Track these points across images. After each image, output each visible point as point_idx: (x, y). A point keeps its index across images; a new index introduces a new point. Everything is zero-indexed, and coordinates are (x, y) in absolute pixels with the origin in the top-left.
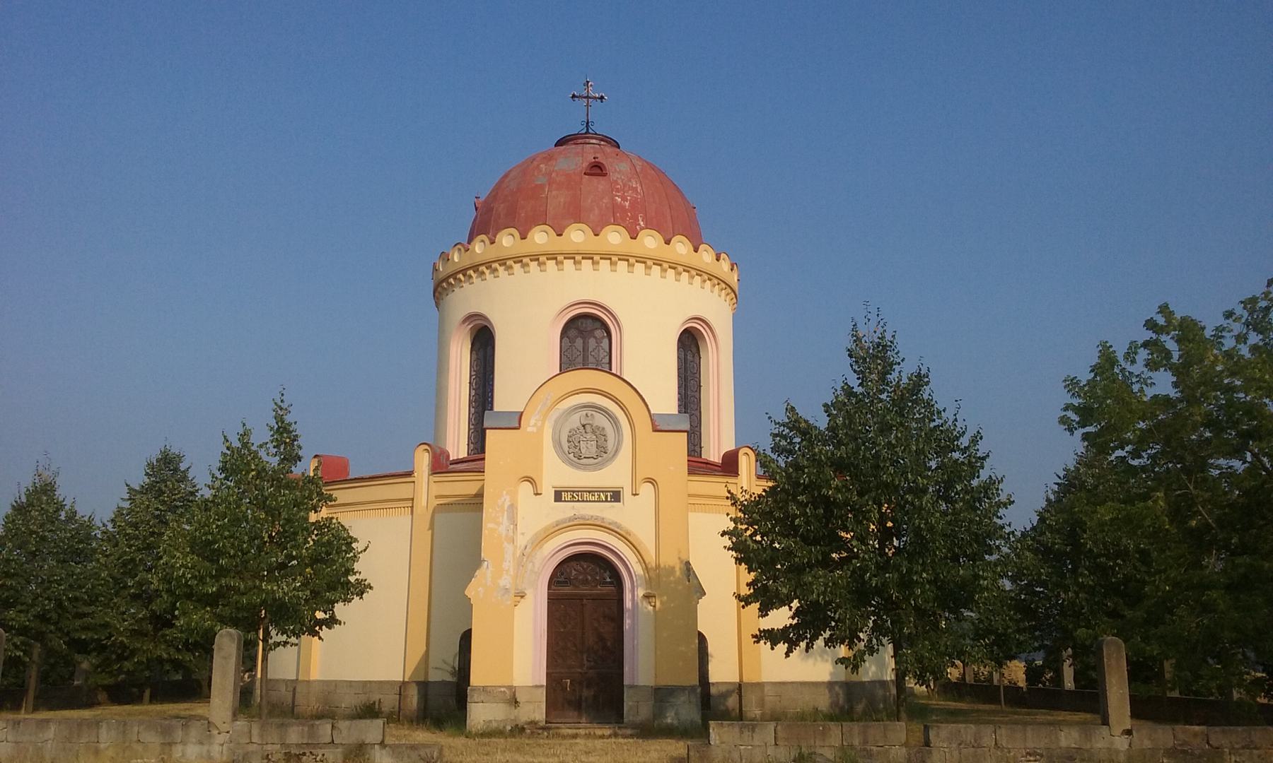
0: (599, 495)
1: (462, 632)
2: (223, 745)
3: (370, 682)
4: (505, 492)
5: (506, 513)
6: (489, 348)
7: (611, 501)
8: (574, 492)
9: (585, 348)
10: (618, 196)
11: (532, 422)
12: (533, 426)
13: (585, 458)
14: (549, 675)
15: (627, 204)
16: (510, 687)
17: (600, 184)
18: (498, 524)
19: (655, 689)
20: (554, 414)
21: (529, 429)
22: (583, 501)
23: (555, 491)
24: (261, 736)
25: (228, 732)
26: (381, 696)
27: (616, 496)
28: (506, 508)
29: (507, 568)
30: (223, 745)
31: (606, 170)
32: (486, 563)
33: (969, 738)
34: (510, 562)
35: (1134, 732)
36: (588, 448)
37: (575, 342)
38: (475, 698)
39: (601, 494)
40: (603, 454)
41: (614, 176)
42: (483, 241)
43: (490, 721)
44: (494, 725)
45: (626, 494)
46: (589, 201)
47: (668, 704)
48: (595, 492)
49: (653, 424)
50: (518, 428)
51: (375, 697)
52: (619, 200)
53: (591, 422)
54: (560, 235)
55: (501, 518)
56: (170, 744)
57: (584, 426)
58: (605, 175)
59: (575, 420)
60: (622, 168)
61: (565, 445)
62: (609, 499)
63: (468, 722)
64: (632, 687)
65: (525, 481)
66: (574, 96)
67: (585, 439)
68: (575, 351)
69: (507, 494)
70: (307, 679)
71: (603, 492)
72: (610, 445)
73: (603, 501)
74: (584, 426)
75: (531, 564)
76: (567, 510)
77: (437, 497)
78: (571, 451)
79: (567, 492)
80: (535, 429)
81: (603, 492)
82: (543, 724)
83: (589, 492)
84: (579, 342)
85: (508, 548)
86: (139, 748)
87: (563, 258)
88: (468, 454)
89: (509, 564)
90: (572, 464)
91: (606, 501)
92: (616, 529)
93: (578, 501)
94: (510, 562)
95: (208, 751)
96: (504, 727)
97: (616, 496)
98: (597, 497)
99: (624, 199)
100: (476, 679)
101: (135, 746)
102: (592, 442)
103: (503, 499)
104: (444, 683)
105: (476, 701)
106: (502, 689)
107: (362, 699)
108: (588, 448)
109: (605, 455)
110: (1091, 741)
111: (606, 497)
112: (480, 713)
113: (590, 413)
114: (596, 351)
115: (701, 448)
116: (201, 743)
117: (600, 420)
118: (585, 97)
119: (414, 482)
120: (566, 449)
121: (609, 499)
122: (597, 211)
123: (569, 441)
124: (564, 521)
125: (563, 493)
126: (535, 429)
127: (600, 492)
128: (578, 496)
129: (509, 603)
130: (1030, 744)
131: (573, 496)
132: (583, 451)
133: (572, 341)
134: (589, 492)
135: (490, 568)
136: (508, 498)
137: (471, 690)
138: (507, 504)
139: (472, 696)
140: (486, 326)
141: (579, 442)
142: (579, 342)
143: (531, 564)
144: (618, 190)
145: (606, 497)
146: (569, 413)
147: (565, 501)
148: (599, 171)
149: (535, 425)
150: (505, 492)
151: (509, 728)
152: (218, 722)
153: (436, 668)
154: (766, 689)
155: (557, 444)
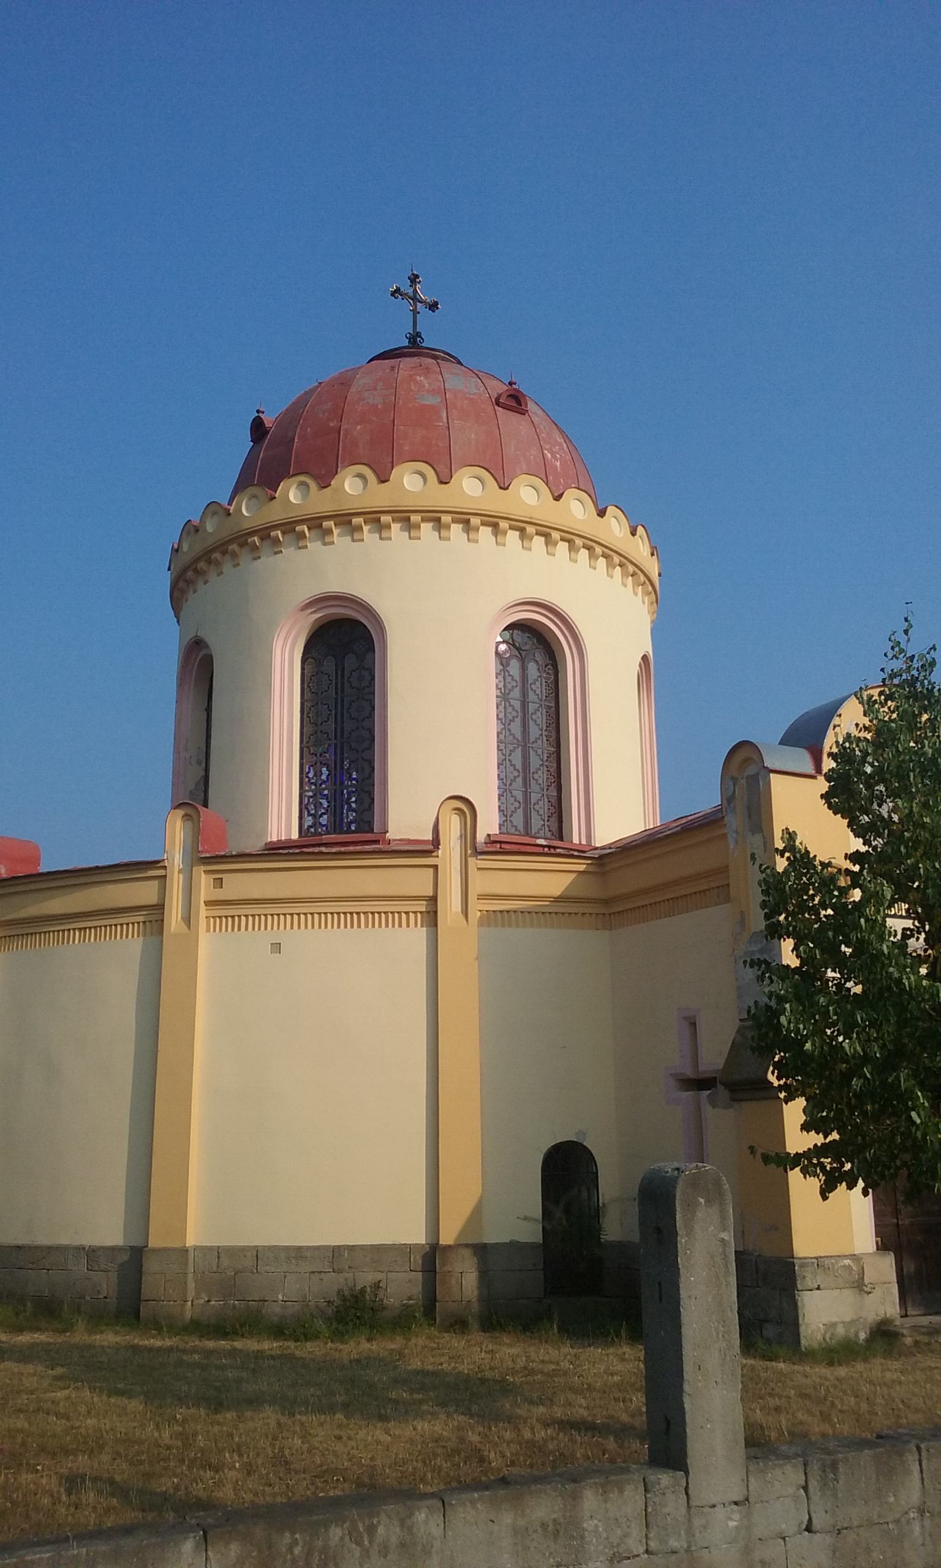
1: (545, 1150)
3: (351, 1248)
6: (350, 662)
16: (855, 1257)
26: (379, 1276)
31: (526, 406)
37: (508, 665)
38: (810, 1282)
42: (360, 476)
43: (834, 1325)
44: (841, 1331)
51: (366, 1278)
58: (523, 413)
63: (802, 1329)
68: (509, 679)
70: (177, 1245)
77: (482, 897)
96: (857, 1335)
106: (847, 1262)
107: (332, 1283)
119: (436, 867)
148: (515, 405)
151: (862, 1336)
153: (525, 1218)
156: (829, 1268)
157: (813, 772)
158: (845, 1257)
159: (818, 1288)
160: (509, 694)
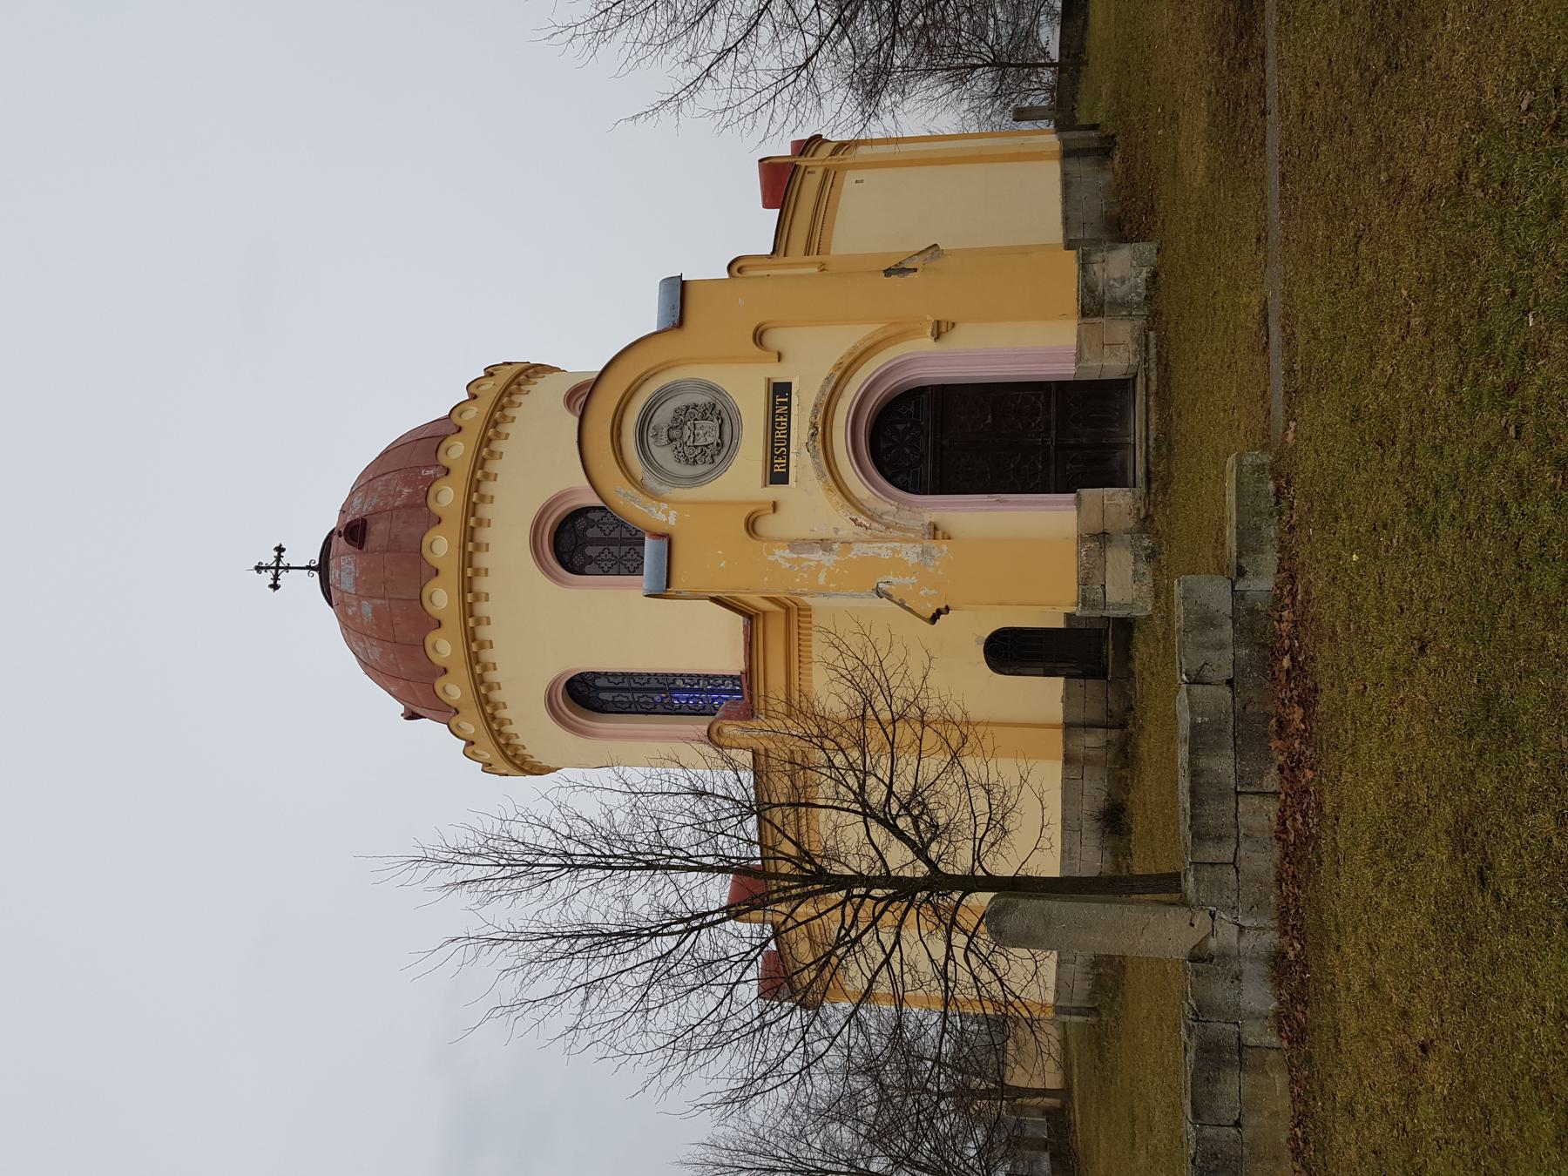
0: (780, 414)
2: (1241, 929)
4: (771, 558)
5: (803, 556)
8: (773, 454)
9: (596, 542)
11: (661, 517)
12: (667, 516)
13: (720, 438)
15: (406, 491)
16: (1081, 539)
17: (377, 533)
18: (820, 566)
20: (652, 483)
21: (672, 521)
22: (788, 439)
23: (771, 483)
24: (1220, 838)
25: (1213, 916)
27: (780, 391)
28: (796, 556)
29: (890, 551)
30: (1241, 929)
32: (880, 585)
34: (880, 548)
36: (707, 432)
37: (591, 557)
39: (777, 412)
40: (718, 412)
45: (780, 374)
47: (1108, 295)
53: (665, 430)
55: (811, 563)
56: (1241, 1047)
57: (671, 440)
59: (663, 454)
61: (700, 469)
62: (786, 400)
65: (755, 533)
67: (692, 439)
69: (773, 554)
71: (774, 410)
72: (703, 399)
75: (885, 517)
76: (801, 460)
78: (709, 459)
79: (773, 464)
80: (673, 513)
82: (1141, 490)
83: (774, 430)
84: (592, 551)
85: (858, 550)
86: (1251, 1121)
87: (469, 569)
89: (884, 551)
90: (729, 458)
91: (789, 404)
92: (833, 384)
93: (788, 447)
94: (880, 548)
95: (1252, 960)
97: (780, 391)
98: (782, 419)
101: (1247, 1133)
102: (698, 426)
103: (781, 561)
104: (1067, 699)
105: (1101, 595)
108: (707, 432)
109: (719, 407)
111: (781, 404)
114: (604, 527)
116: (1238, 977)
117: (664, 416)
120: (707, 467)
121: (786, 400)
123: (695, 462)
124: (817, 466)
125: (775, 470)
126: (673, 513)
127: (774, 414)
128: (779, 447)
129: (944, 547)
131: (781, 455)
132: (710, 440)
133: (591, 560)
134: (774, 430)
135: (891, 578)
136: (779, 553)
138: (788, 554)
140: (568, 684)
141: (696, 447)
142: (592, 551)
143: (885, 517)
145: (781, 404)
146: (651, 464)
147: (787, 467)
149: (666, 513)
150: (771, 558)
152: (1194, 937)
155: (696, 480)
156: (1088, 573)
157: (666, 540)
158: (1078, 552)
159: (1104, 586)
160: (615, 557)
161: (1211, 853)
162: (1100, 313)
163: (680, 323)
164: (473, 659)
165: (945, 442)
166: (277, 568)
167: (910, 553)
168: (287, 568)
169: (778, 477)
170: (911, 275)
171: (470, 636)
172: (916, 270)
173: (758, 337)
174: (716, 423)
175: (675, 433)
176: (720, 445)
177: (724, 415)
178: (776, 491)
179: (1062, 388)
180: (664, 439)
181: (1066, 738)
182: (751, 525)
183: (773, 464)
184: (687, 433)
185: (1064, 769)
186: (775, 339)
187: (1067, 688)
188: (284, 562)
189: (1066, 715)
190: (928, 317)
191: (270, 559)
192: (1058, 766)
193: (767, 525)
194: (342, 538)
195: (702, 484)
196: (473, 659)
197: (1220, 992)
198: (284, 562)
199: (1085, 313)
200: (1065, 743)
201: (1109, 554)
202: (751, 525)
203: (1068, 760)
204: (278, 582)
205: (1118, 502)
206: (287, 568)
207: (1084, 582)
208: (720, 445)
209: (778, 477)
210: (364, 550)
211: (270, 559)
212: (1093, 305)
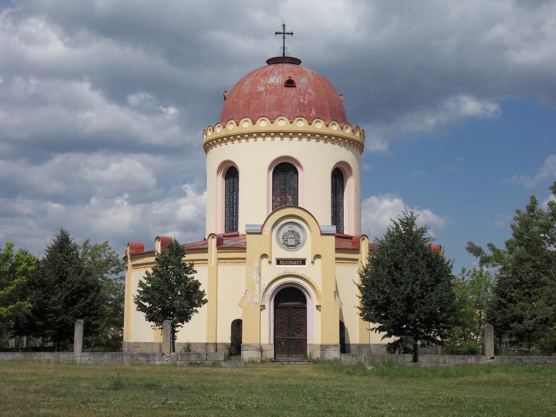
0: (296, 262)
4: (255, 261)
7: (301, 265)
8: (285, 260)
10: (302, 98)
14: (275, 339)
15: (306, 102)
17: (292, 91)
19: (321, 345)
25: (169, 357)
27: (303, 262)
28: (256, 268)
33: (435, 360)
35: (495, 358)
38: (245, 348)
40: (297, 244)
41: (299, 86)
46: (287, 101)
47: (326, 352)
48: (294, 260)
49: (321, 231)
50: (260, 233)
52: (302, 100)
54: (272, 123)
57: (289, 231)
58: (295, 86)
59: (286, 229)
60: (303, 82)
61: (281, 240)
64: (310, 345)
66: (276, 33)
71: (298, 260)
72: (301, 240)
73: (298, 265)
74: (289, 231)
78: (284, 242)
79: (282, 260)
81: (298, 260)
82: (273, 360)
83: (292, 260)
88: (225, 233)
89: (257, 292)
93: (287, 264)
97: (303, 262)
99: (305, 100)
100: (245, 340)
103: (254, 264)
106: (256, 345)
109: (299, 245)
110: (479, 361)
111: (299, 263)
112: (246, 355)
113: (292, 225)
115: (343, 228)
117: (296, 229)
118: (282, 33)
122: (290, 107)
123: (283, 238)
128: (287, 262)
130: (457, 362)
134: (292, 260)
136: (257, 263)
137: (242, 345)
138: (256, 266)
139: (243, 348)
144: (301, 95)
145: (299, 263)
147: (281, 265)
152: (166, 354)
154: (372, 347)
155: (278, 239)
161: (179, 357)
162: (321, 350)
163: (322, 234)
164: (242, 136)
165: (290, 308)
166: (284, 33)
167: (256, 299)
168: (284, 38)
169: (279, 262)
170: (334, 299)
171: (250, 135)
172: (335, 300)
173: (318, 256)
174: (294, 244)
175: (291, 233)
176: (288, 246)
177: (297, 246)
178: (274, 262)
179: (304, 340)
180: (290, 229)
181: (213, 344)
182: (264, 256)
183: (282, 260)
184: (291, 236)
185: (204, 343)
186: (318, 261)
187: (229, 344)
188: (286, 36)
189: (220, 344)
190: (322, 303)
191: (288, 30)
192: (205, 342)
193: (265, 261)
194: (289, 79)
195: (277, 241)
196: (242, 136)
197: (157, 358)
198: (286, 36)
199: (321, 346)
200: (211, 343)
201: (255, 352)
202: (264, 256)
203: (207, 344)
204: (278, 34)
205: (270, 354)
206: (284, 38)
207: (248, 345)
208: (288, 246)
209: (279, 262)
210: (284, 87)
211: (288, 30)
212: (324, 348)
